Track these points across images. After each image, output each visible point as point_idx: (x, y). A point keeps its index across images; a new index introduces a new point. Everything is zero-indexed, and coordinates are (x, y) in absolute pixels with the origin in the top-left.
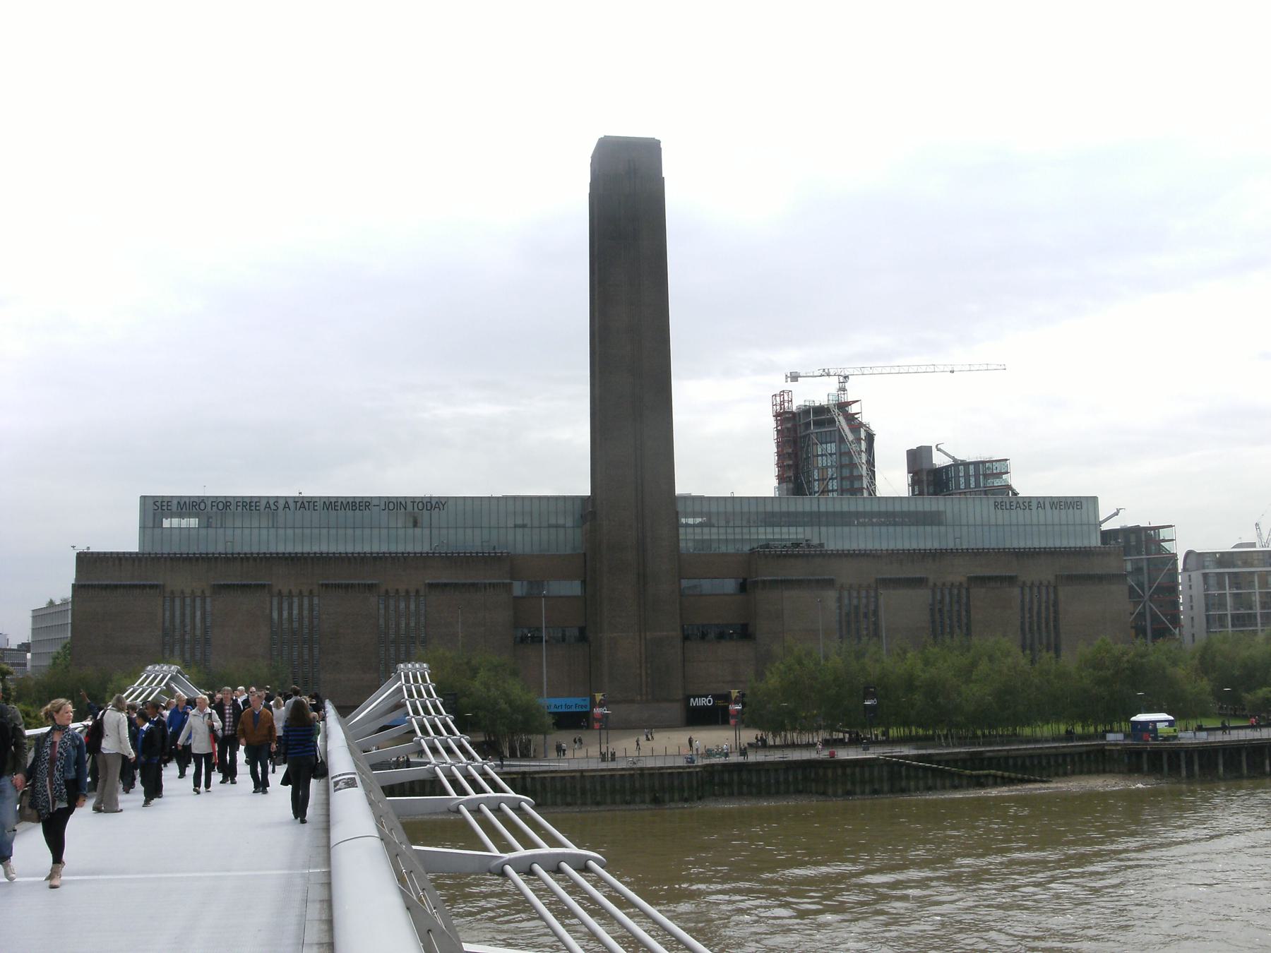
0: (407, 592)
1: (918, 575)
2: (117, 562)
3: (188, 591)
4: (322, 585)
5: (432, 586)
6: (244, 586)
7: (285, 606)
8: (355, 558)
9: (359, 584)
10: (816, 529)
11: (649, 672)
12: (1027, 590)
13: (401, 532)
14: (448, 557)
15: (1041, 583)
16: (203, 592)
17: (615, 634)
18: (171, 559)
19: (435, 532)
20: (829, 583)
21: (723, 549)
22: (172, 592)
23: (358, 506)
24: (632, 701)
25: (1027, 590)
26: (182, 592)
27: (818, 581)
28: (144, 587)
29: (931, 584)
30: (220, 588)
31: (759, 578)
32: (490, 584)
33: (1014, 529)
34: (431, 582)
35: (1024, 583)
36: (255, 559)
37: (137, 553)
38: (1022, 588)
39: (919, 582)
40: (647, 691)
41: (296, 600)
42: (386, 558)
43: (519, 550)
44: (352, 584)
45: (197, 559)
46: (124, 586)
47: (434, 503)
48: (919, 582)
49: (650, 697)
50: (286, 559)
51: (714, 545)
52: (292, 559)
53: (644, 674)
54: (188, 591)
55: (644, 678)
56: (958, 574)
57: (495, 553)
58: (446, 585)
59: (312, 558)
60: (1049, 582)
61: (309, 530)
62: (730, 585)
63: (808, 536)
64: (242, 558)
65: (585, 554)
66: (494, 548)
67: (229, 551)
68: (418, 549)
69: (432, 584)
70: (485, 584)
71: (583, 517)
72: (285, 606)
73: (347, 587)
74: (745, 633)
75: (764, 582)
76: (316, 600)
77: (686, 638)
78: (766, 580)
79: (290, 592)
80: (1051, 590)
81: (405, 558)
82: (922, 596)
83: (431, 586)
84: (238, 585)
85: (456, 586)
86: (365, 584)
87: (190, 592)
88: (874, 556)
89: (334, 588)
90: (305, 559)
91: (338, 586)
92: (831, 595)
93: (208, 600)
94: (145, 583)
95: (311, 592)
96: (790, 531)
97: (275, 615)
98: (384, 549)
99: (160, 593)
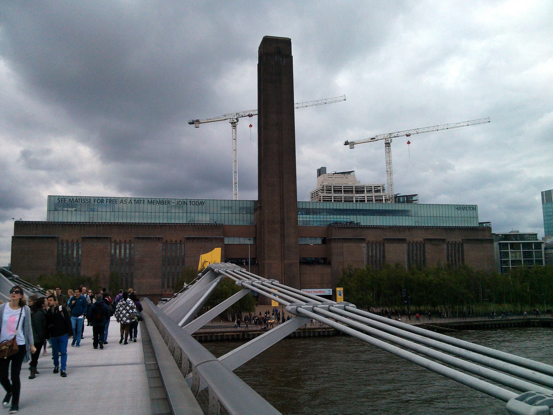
0: (176, 241)
1: (401, 238)
2: (35, 226)
3: (70, 240)
4: (136, 237)
5: (188, 239)
6: (96, 238)
7: (118, 246)
9: (153, 238)
10: (355, 216)
12: (450, 246)
13: (181, 214)
15: (456, 242)
16: (77, 241)
18: (62, 225)
19: (189, 215)
20: (363, 240)
21: (315, 224)
22: (62, 241)
23: (164, 202)
25: (450, 246)
26: (67, 241)
27: (358, 239)
28: (48, 238)
29: (408, 242)
30: (84, 239)
31: (333, 237)
32: (214, 238)
33: (441, 218)
34: (187, 237)
35: (449, 242)
36: (103, 225)
37: (45, 222)
38: (448, 244)
39: (403, 241)
41: (123, 245)
43: (226, 223)
44: (150, 237)
46: (38, 238)
47: (199, 202)
48: (403, 241)
50: (119, 225)
51: (311, 223)
53: (283, 279)
54: (70, 240)
56: (419, 237)
57: (217, 224)
58: (194, 238)
60: (459, 242)
61: (138, 213)
62: (319, 241)
63: (352, 220)
65: (256, 226)
66: (216, 222)
67: (91, 221)
68: (181, 222)
70: (212, 238)
71: (255, 210)
72: (118, 246)
73: (148, 238)
74: (326, 261)
76: (133, 245)
77: (301, 263)
79: (120, 241)
80: (460, 245)
81: (175, 226)
82: (405, 246)
83: (187, 238)
85: (199, 238)
86: (156, 237)
87: (71, 241)
88: (383, 229)
90: (128, 225)
91: (144, 238)
92: (365, 245)
93: (80, 245)
94: (49, 236)
95: (130, 241)
96: (327, 217)
97: (113, 251)
98: (165, 222)
99: (56, 241)
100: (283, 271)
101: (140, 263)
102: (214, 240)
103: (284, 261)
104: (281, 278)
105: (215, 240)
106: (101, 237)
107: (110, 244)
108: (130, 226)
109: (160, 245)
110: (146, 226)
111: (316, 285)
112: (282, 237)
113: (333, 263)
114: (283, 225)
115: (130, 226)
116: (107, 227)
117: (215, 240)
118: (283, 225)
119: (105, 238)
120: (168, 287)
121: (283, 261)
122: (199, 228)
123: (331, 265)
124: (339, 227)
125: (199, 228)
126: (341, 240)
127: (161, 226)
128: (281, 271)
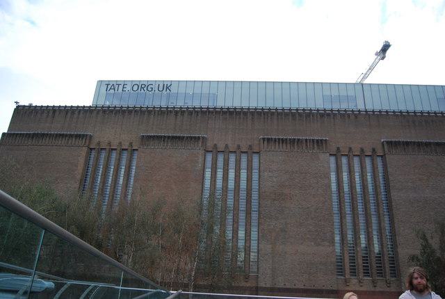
0: (362, 150)
2: (51, 114)
4: (264, 139)
6: (174, 138)
8: (299, 114)
16: (131, 144)
22: (99, 144)
26: (109, 144)
28: (71, 136)
30: (147, 139)
36: (191, 113)
42: (335, 115)
44: (299, 140)
45: (130, 112)
50: (225, 113)
52: (231, 113)
58: (407, 143)
59: (252, 113)
64: (177, 113)
69: (391, 142)
73: (292, 141)
81: (356, 116)
83: (389, 143)
84: (169, 137)
89: (277, 143)
90: (245, 114)
101: (274, 200)
106: (184, 137)
107: (201, 152)
108: (250, 117)
109: (323, 157)
110: (287, 114)
115: (250, 117)
116: (199, 118)
119: (191, 138)
120: (354, 272)
122: (414, 122)
125: (414, 122)
127: (322, 115)
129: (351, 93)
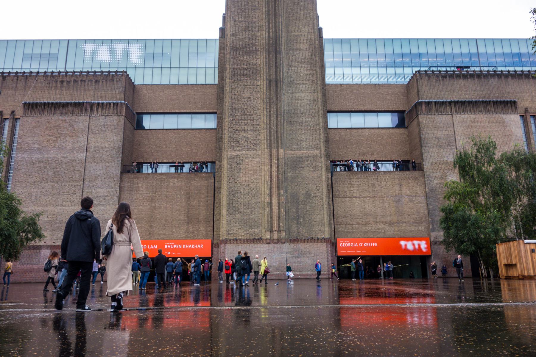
11: (282, 199)
14: (54, 76)
17: (237, 153)
24: (259, 240)
32: (98, 104)
40: (279, 226)
49: (283, 235)
55: (275, 208)
69: (29, 104)
70: (92, 105)
75: (428, 104)
78: (432, 102)
100: (275, 179)
102: (98, 109)
103: (278, 151)
104: (267, 200)
105: (100, 109)
111: (379, 226)
112: (273, 88)
113: (427, 166)
114: (276, 58)
117: (100, 109)
118: (276, 58)
121: (274, 151)
122: (62, 82)
123: (421, 169)
124: (437, 76)
126: (448, 108)
128: (267, 177)
129: (54, 51)
